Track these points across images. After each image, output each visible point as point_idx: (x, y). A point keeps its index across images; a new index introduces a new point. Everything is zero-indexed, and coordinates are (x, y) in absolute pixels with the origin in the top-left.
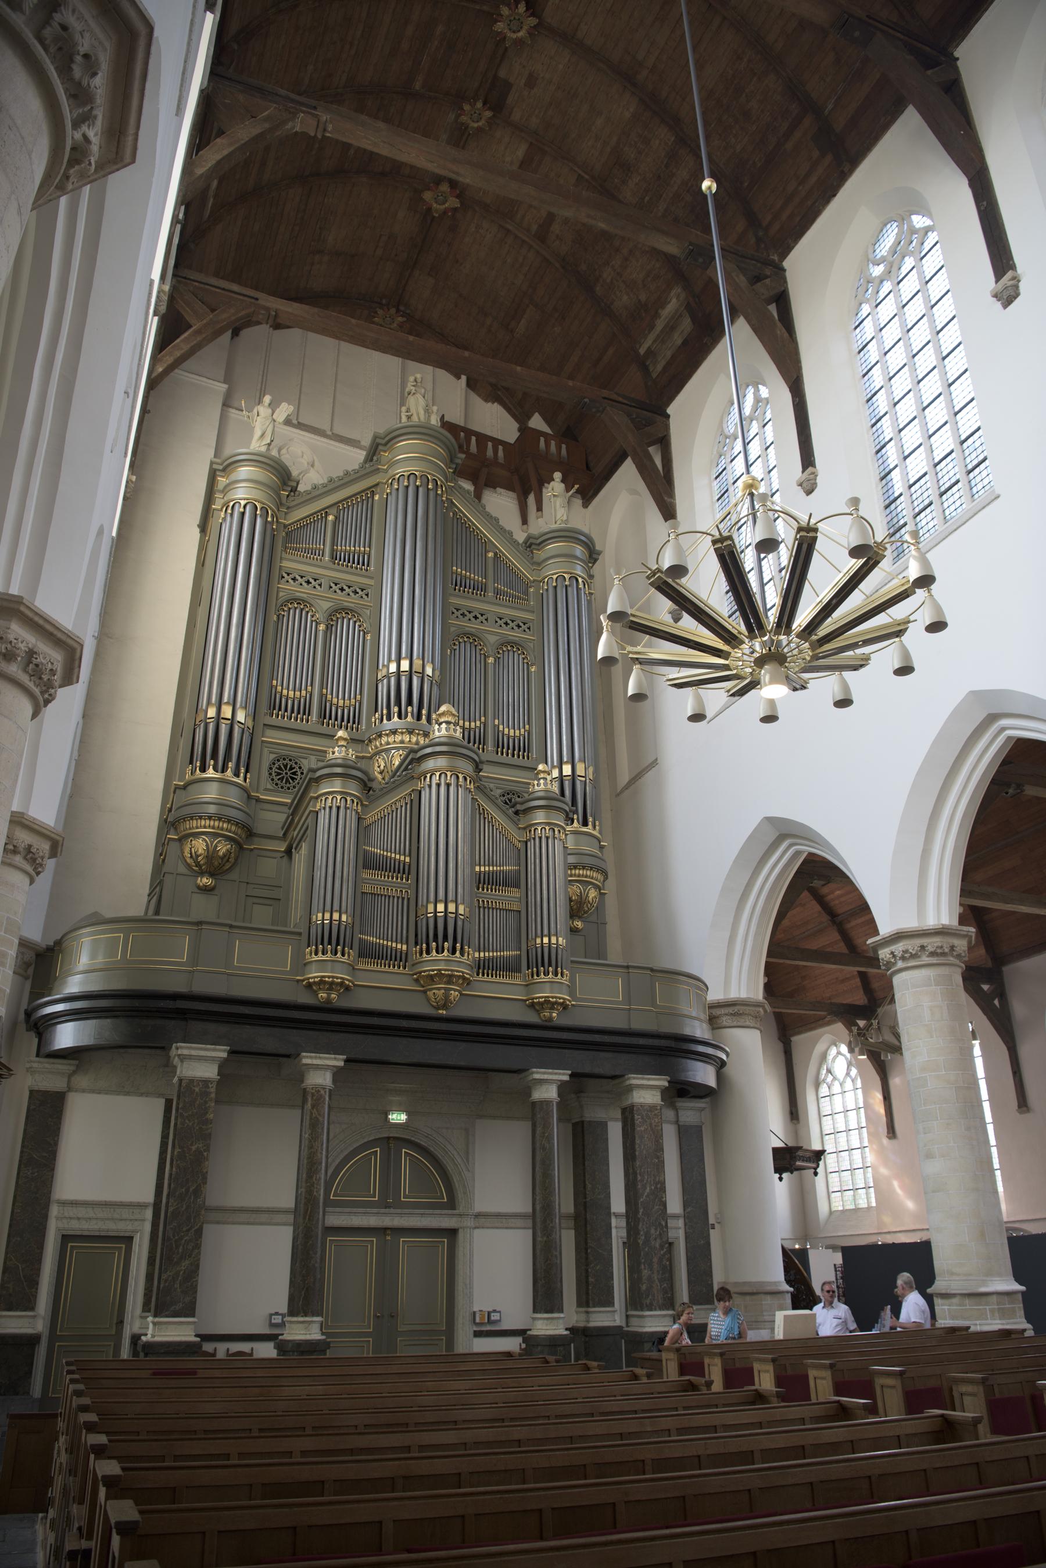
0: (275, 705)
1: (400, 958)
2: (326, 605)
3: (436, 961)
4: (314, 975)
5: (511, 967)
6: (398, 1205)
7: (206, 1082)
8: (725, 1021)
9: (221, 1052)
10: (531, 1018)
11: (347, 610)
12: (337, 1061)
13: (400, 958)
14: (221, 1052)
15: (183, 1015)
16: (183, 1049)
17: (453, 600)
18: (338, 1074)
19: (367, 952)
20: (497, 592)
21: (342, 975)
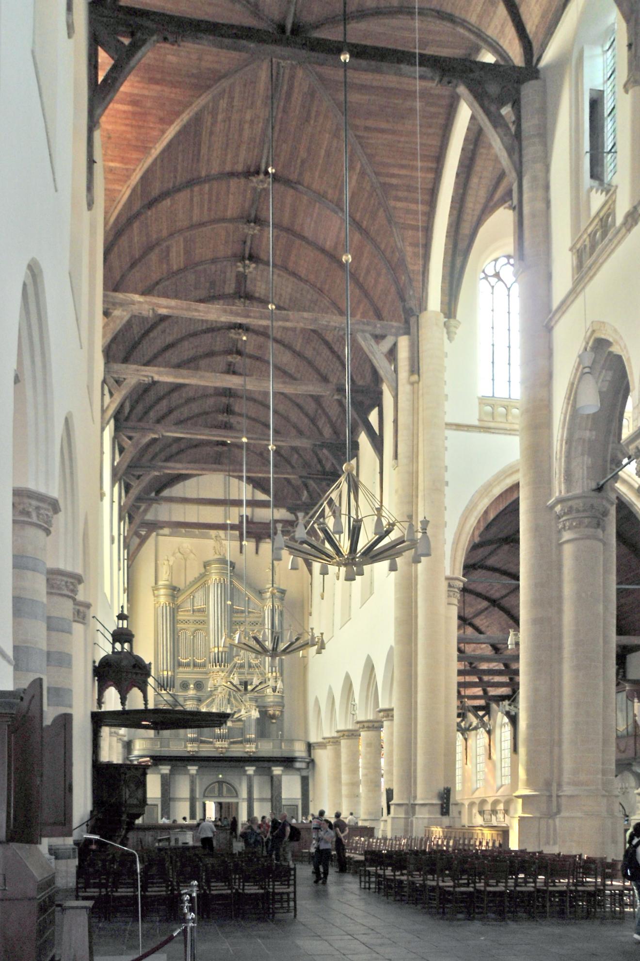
0: (180, 665)
1: (211, 743)
2: (193, 629)
3: (218, 744)
4: (189, 749)
5: (241, 742)
6: (223, 796)
7: (166, 774)
8: (316, 747)
9: (169, 767)
10: (246, 755)
11: (198, 630)
12: (196, 768)
13: (211, 743)
14: (169, 767)
15: (160, 760)
16: (161, 767)
17: (234, 619)
18: (197, 771)
19: (202, 742)
20: (249, 612)
21: (196, 749)
